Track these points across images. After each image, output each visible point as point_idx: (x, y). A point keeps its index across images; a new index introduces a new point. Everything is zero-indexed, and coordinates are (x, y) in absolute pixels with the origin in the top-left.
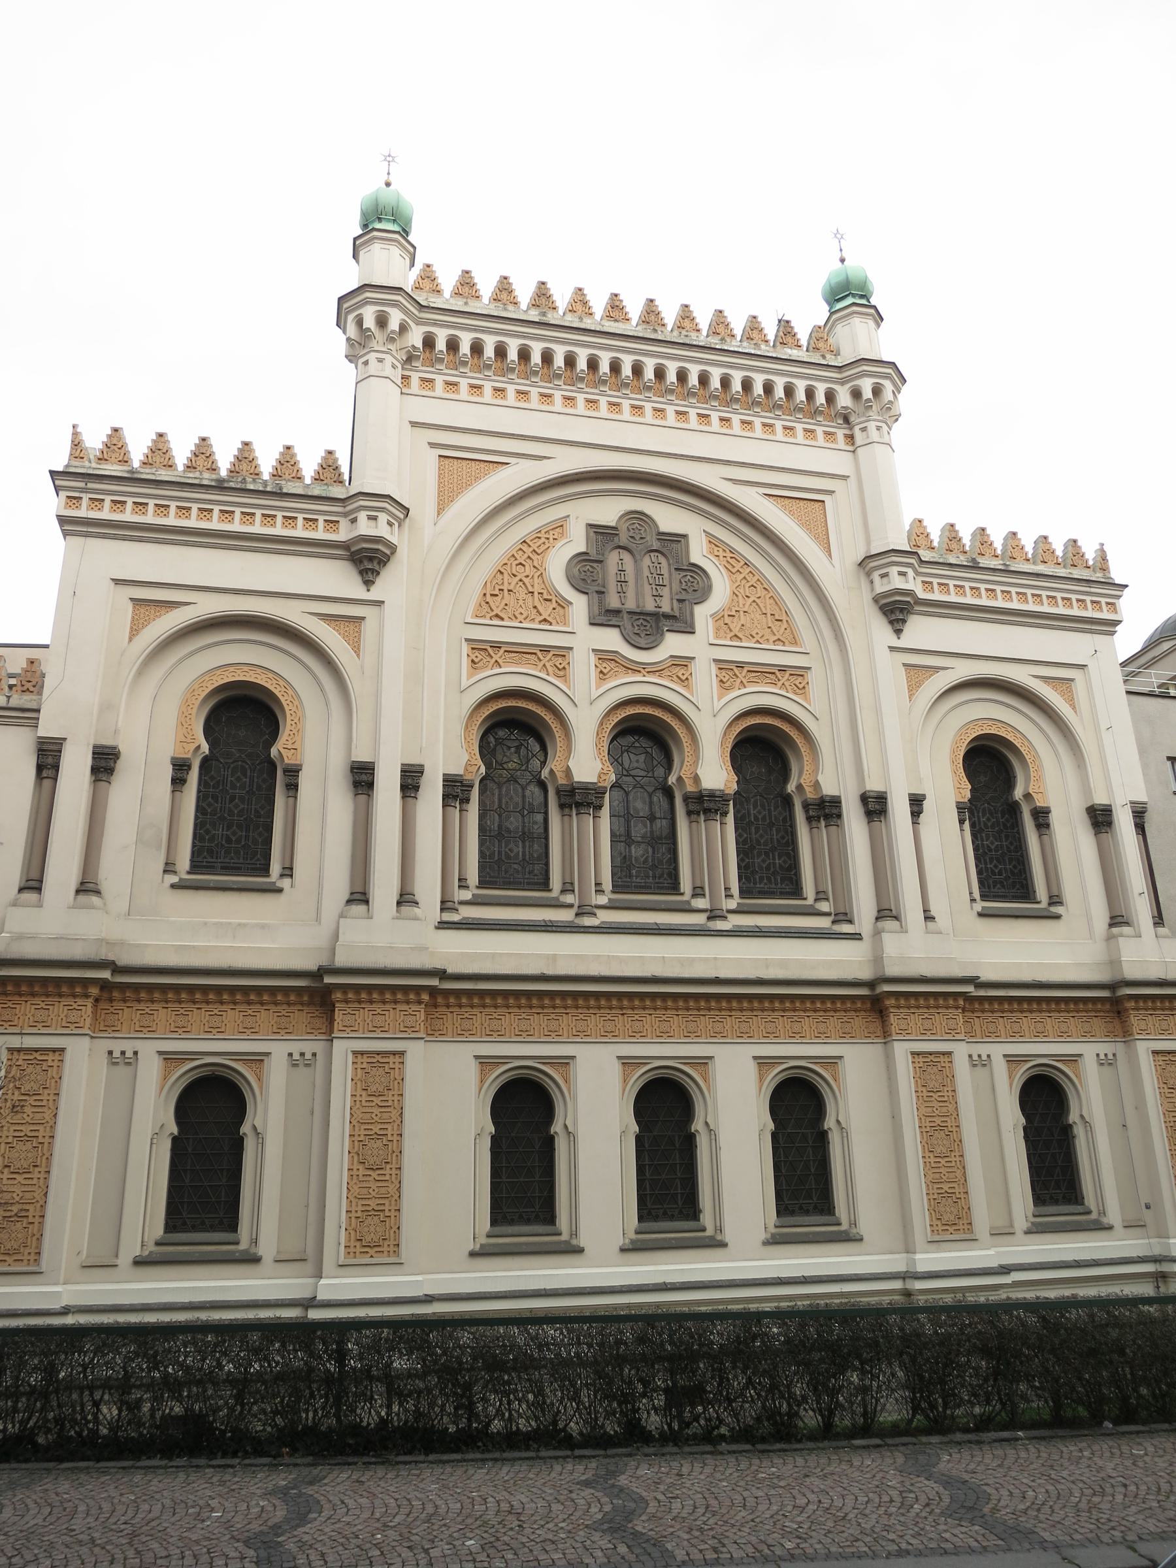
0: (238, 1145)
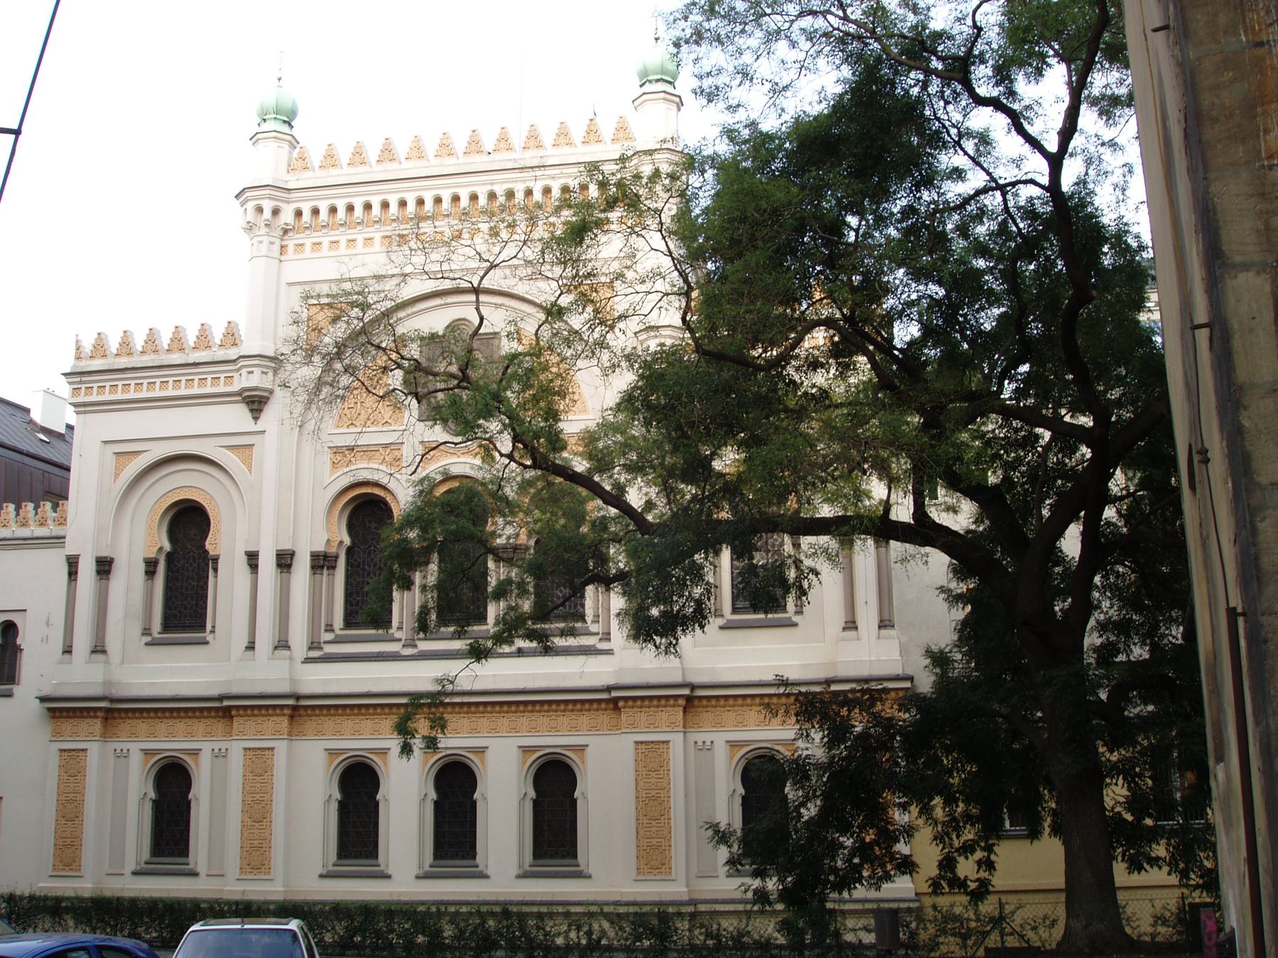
0: (188, 804)
